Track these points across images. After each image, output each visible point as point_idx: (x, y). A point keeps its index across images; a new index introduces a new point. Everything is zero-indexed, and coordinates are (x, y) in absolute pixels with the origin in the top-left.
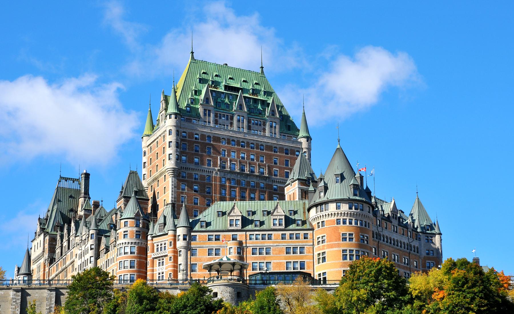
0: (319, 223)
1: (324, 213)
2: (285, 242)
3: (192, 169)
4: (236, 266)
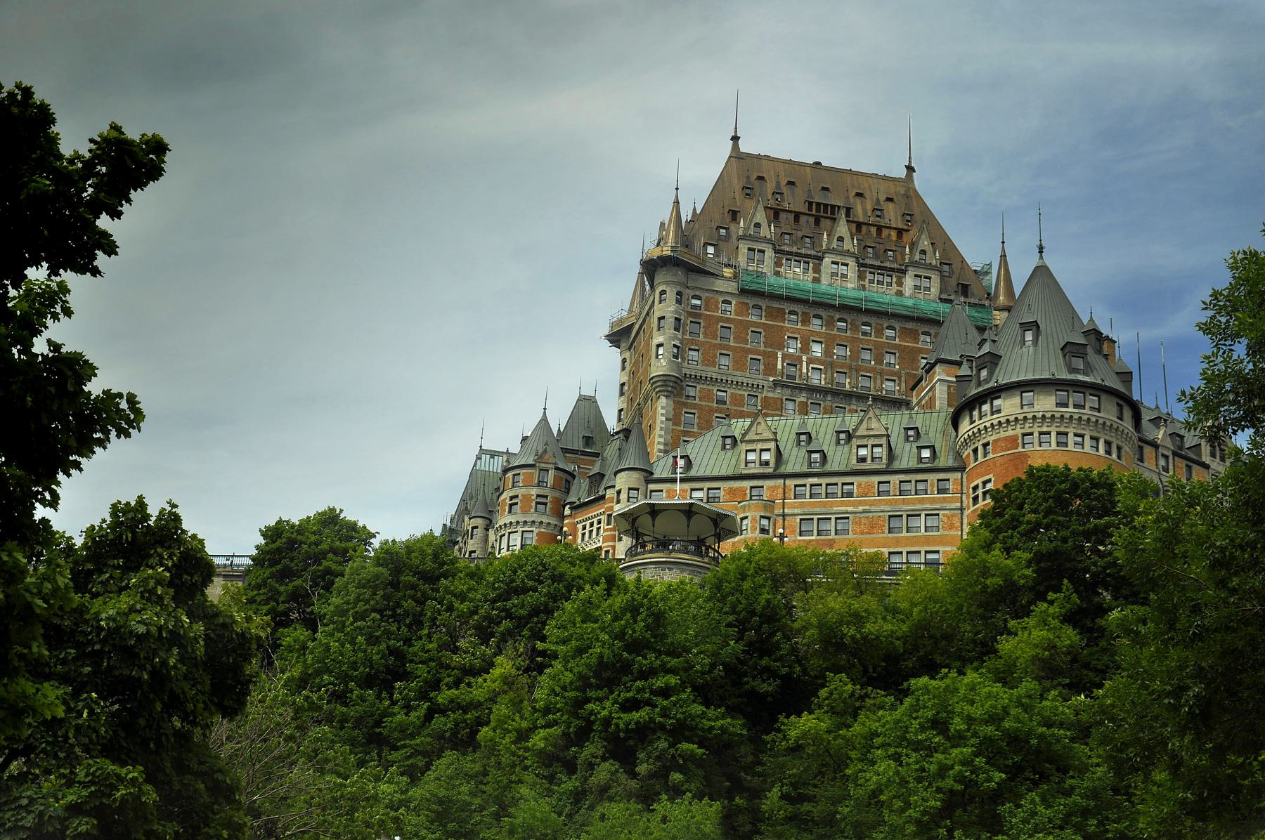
0: (975, 451)
2: (887, 503)
3: (711, 378)
4: (695, 519)
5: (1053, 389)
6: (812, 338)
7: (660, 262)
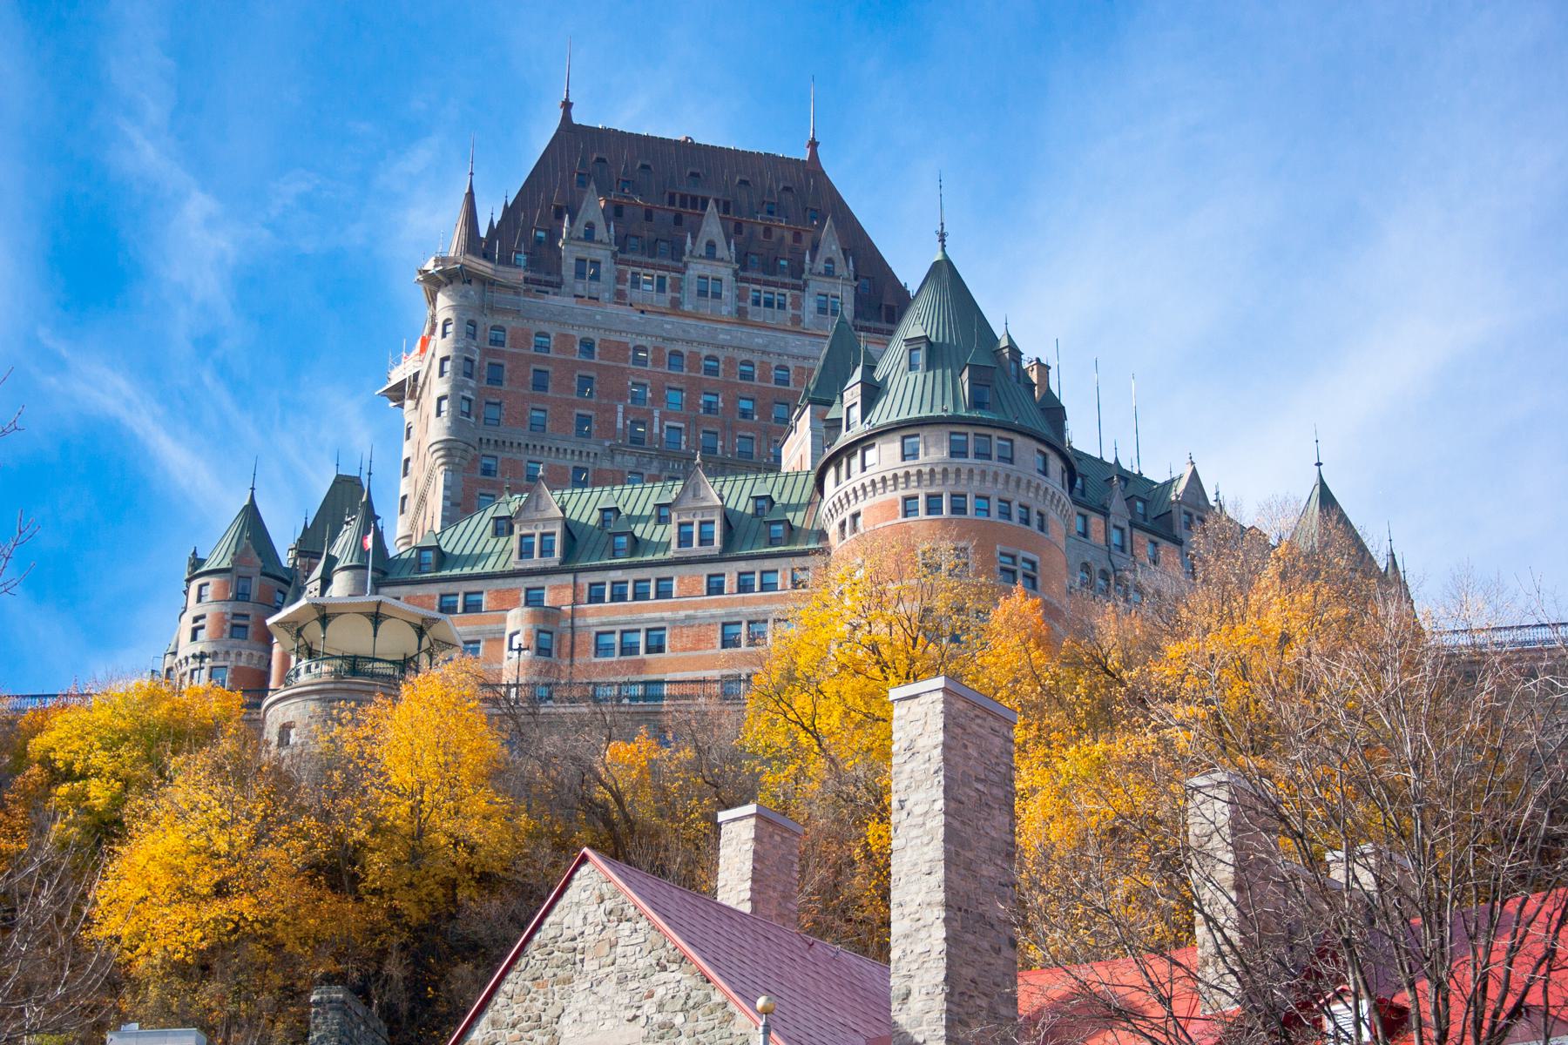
2: (720, 604)
3: (519, 444)
4: (384, 627)
6: (667, 384)
7: (440, 277)
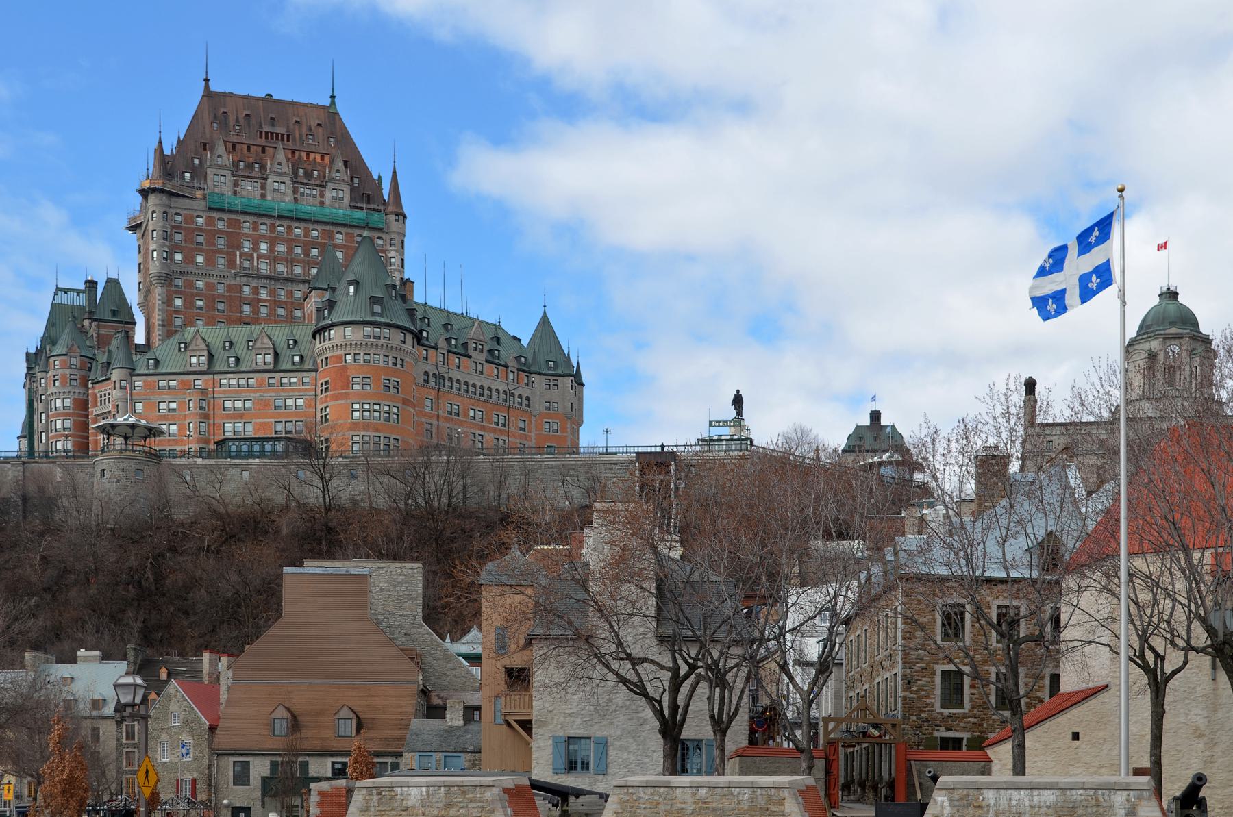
0: (322, 360)
1: (327, 344)
2: (273, 391)
4: (137, 430)
5: (362, 326)
